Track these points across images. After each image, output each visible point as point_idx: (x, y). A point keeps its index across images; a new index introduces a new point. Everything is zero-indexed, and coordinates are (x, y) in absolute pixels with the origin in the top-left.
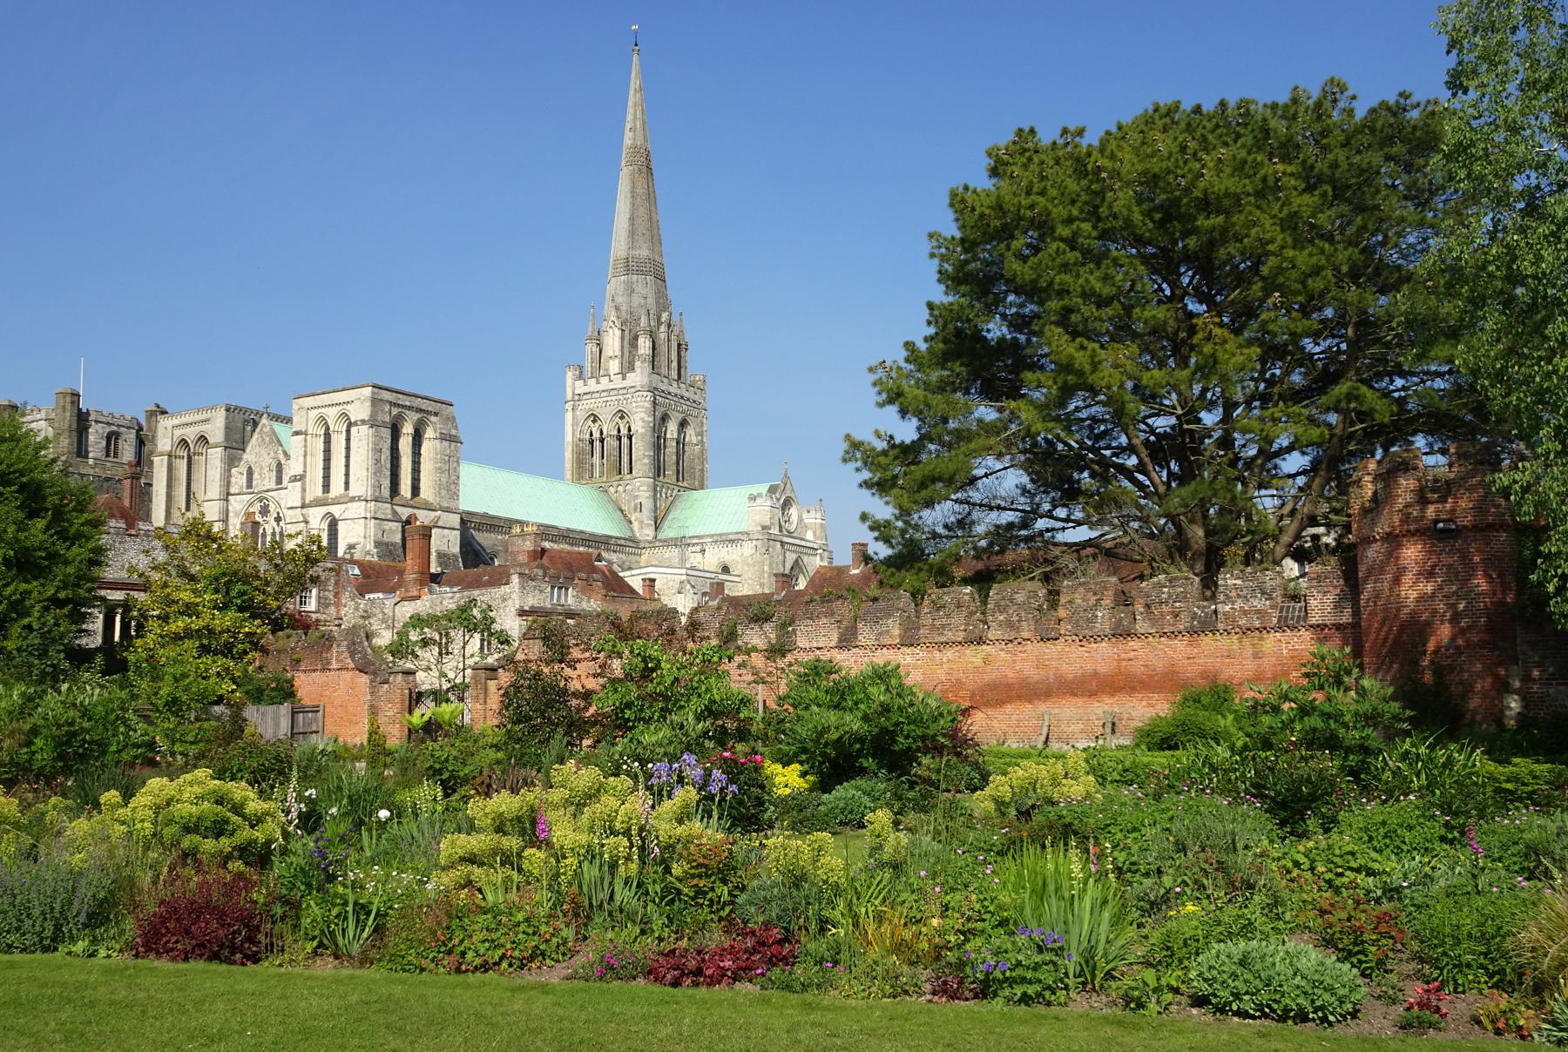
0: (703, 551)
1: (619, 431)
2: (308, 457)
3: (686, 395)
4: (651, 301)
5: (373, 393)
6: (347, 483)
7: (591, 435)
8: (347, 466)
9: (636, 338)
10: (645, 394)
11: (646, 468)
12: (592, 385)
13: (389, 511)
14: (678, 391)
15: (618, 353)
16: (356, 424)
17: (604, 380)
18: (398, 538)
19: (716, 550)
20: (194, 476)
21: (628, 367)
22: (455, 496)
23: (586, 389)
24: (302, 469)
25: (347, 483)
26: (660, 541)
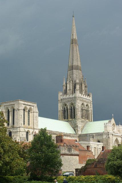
0: (93, 137)
1: (71, 108)
3: (87, 98)
9: (75, 85)
12: (65, 97)
18: (25, 136)
22: (37, 126)
25: (13, 124)
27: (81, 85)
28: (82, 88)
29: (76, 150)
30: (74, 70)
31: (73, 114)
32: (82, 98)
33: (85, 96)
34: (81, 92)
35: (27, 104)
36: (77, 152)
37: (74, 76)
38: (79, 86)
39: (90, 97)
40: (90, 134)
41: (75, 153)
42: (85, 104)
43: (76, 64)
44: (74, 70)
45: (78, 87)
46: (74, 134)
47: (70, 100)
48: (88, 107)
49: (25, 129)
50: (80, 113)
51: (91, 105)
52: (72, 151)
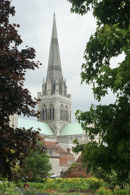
1: (51, 109)
3: (67, 99)
7: (44, 109)
9: (55, 86)
14: (65, 99)
17: (47, 96)
21: (53, 92)
26: (61, 136)
27: (61, 86)
28: (61, 89)
29: (57, 153)
30: (54, 71)
31: (52, 116)
33: (64, 97)
34: (60, 93)
36: (58, 155)
37: (54, 76)
38: (58, 87)
40: (69, 135)
42: (65, 105)
43: (57, 64)
44: (54, 71)
45: (57, 87)
46: (53, 136)
48: (67, 108)
50: (59, 114)
51: (70, 107)
52: (53, 154)
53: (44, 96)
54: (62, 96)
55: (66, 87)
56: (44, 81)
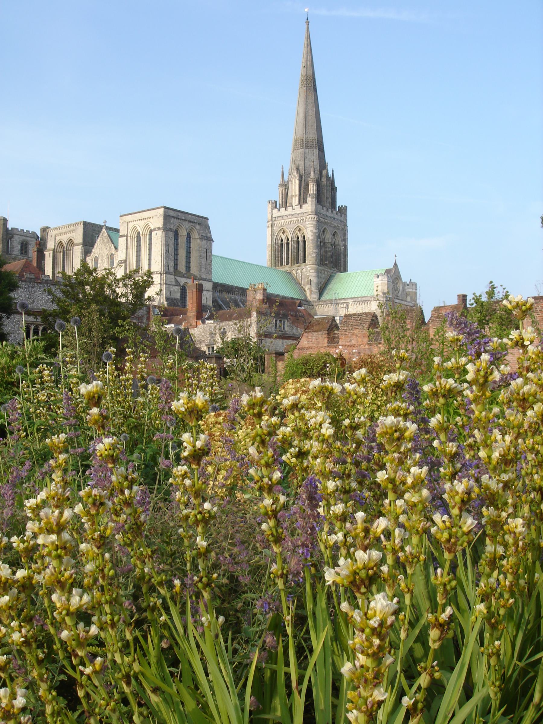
0: (347, 307)
1: (298, 238)
2: (128, 250)
3: (336, 217)
4: (317, 163)
5: (164, 212)
6: (150, 264)
8: (150, 254)
10: (313, 216)
11: (314, 259)
13: (173, 280)
14: (332, 215)
15: (297, 193)
16: (155, 230)
17: (290, 209)
19: (355, 306)
20: (67, 262)
21: (302, 201)
22: (210, 272)
23: (279, 214)
24: (125, 256)
26: (322, 301)
32: (323, 217)
33: (330, 211)
35: (183, 218)
39: (343, 215)
41: (293, 334)
47: (295, 219)
49: (179, 279)
53: (283, 210)
54: (325, 208)
55: (334, 189)
56: (283, 175)
